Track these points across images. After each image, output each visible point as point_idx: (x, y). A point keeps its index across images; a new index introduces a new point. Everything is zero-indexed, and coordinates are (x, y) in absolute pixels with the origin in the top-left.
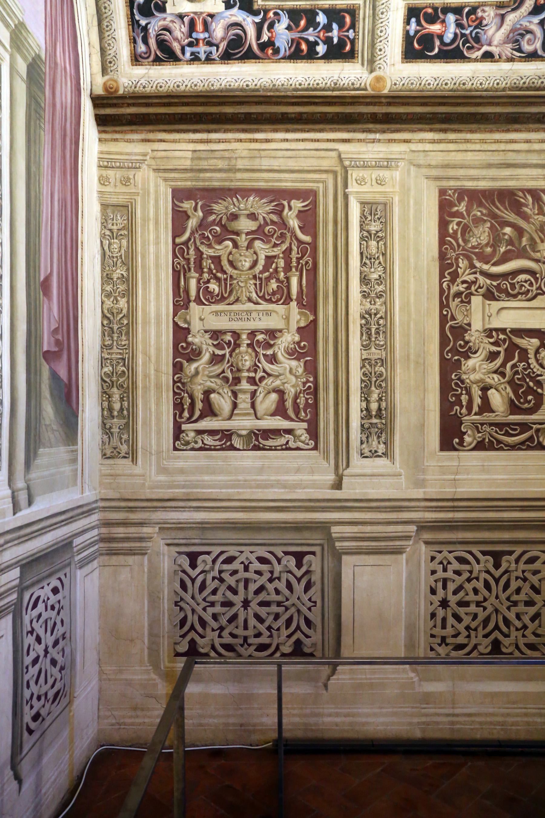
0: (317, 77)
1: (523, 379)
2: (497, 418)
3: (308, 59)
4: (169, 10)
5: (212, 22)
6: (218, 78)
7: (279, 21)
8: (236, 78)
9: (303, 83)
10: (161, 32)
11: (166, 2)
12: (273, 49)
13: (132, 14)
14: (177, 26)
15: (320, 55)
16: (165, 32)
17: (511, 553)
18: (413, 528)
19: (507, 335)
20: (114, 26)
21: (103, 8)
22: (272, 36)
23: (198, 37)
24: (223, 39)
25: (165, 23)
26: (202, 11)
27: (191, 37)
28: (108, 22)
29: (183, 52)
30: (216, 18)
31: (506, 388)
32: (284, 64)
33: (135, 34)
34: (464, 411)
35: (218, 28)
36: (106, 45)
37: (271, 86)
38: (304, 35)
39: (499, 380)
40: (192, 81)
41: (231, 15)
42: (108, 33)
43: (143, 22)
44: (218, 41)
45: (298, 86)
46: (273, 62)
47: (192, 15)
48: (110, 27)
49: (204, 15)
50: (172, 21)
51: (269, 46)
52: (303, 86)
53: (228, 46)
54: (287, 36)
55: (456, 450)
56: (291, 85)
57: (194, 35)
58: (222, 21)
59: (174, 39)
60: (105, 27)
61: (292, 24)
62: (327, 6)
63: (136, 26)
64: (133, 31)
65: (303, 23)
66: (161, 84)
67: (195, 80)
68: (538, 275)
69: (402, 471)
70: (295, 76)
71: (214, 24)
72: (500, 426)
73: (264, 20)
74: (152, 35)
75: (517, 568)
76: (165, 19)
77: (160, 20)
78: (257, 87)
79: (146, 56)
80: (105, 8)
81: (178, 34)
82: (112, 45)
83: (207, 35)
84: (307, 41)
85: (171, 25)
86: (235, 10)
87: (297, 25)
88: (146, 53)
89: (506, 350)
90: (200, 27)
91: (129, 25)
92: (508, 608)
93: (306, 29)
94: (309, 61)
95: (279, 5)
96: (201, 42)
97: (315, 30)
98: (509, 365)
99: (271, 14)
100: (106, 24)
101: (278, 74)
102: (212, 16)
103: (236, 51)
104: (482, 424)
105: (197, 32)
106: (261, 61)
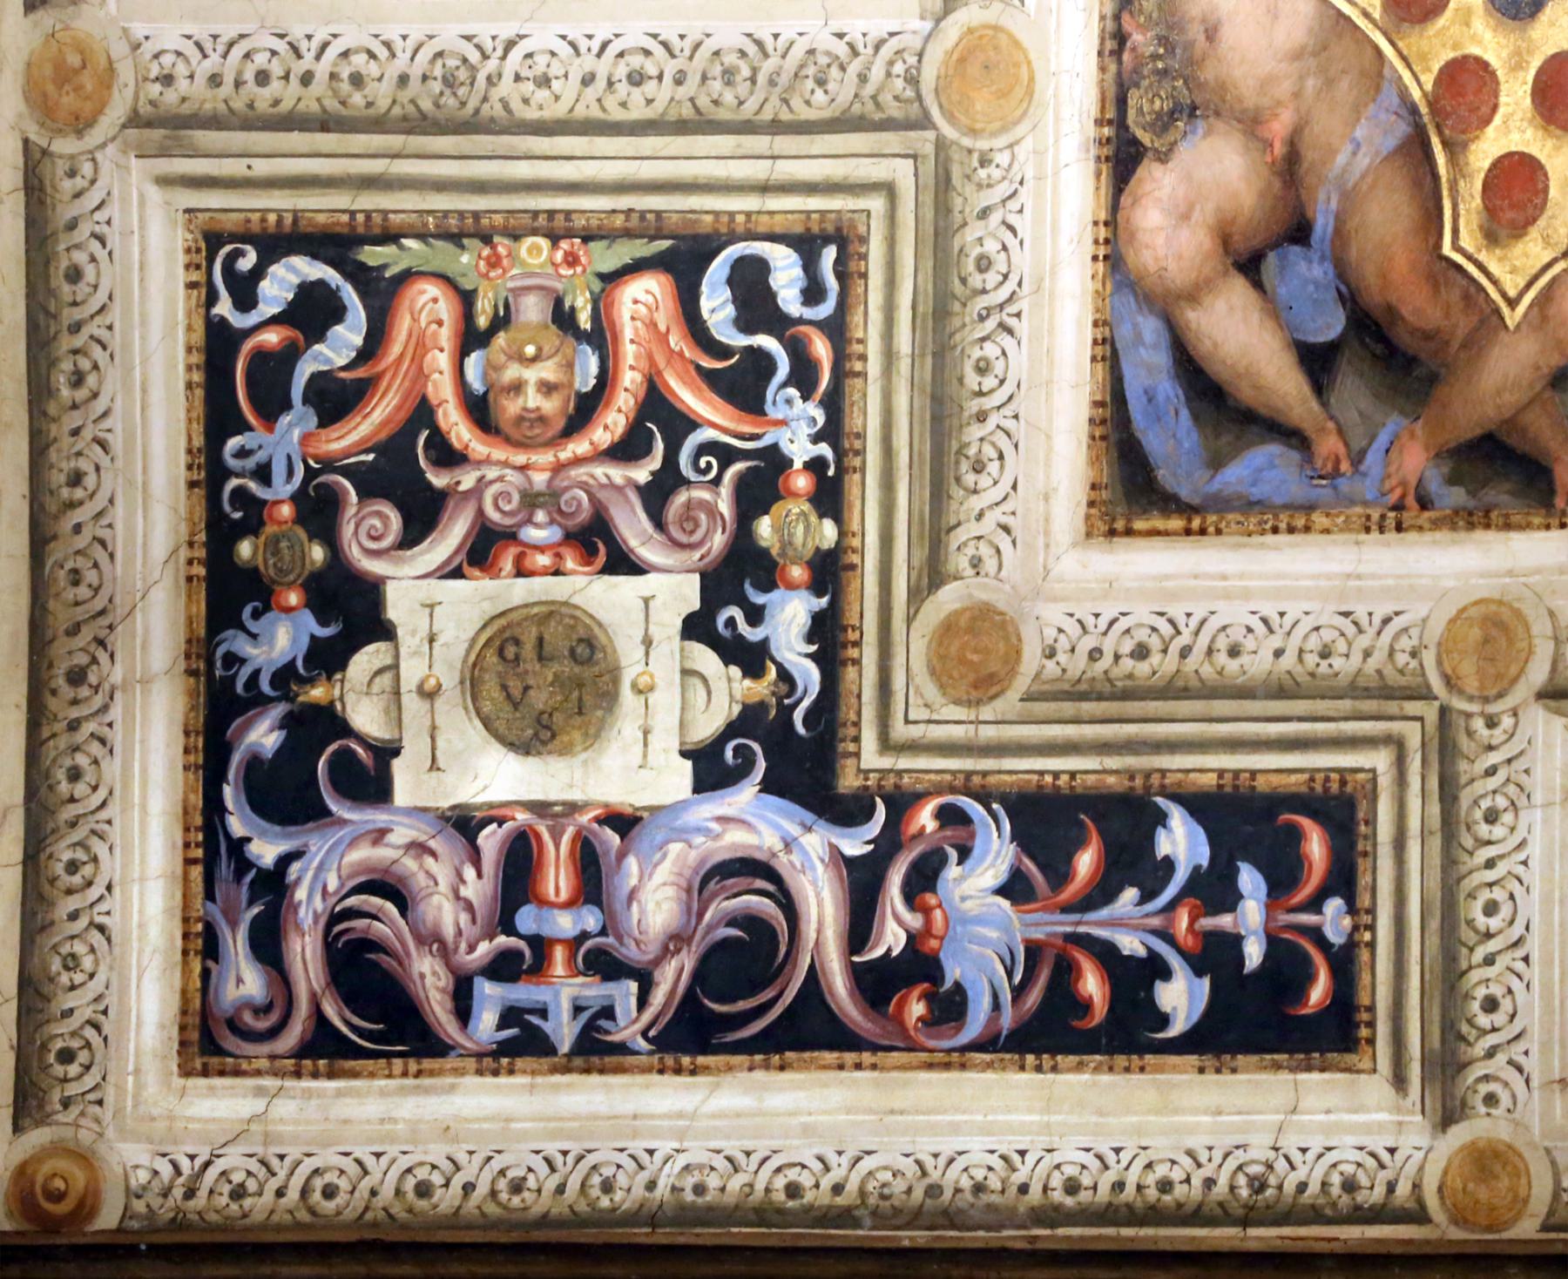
0: (1161, 1147)
3: (1111, 1051)
4: (402, 794)
5: (622, 855)
6: (637, 1146)
7: (964, 853)
8: (733, 1147)
9: (1086, 1181)
10: (352, 901)
11: (396, 752)
12: (929, 997)
13: (214, 808)
14: (442, 871)
15: (1176, 1029)
16: (376, 901)
20: (110, 866)
21: (61, 775)
22: (928, 930)
23: (546, 931)
24: (676, 941)
25: (383, 853)
26: (576, 795)
27: (509, 928)
28: (81, 844)
29: (463, 1010)
30: (646, 836)
32: (990, 1076)
33: (215, 911)
35: (651, 885)
36: (56, 965)
37: (918, 1194)
38: (1094, 924)
40: (496, 1165)
41: (721, 819)
42: (72, 903)
43: (265, 851)
44: (652, 951)
45: (1058, 1196)
46: (930, 1066)
47: (522, 817)
48: (87, 870)
49: (585, 818)
50: (419, 848)
51: (910, 982)
52: (1085, 1196)
53: (698, 976)
54: (1007, 929)
56: (1024, 1189)
57: (527, 918)
58: (675, 848)
59: (421, 940)
60: (59, 869)
61: (1030, 866)
62: (1210, 780)
63: (225, 869)
64: (210, 895)
65: (1086, 862)
66: (330, 1177)
67: (517, 1159)
70: (1044, 1141)
71: (632, 863)
73: (888, 845)
74: (305, 916)
76: (379, 835)
77: (353, 843)
78: (840, 1201)
79: (263, 1024)
80: (75, 775)
81: (443, 913)
82: (87, 963)
83: (591, 919)
84: (1107, 955)
85: (410, 864)
86: (744, 797)
87: (1059, 874)
88: (267, 1009)
90: (557, 878)
91: (189, 862)
93: (1102, 892)
94: (1121, 1060)
95: (969, 774)
96: (559, 953)
97: (1146, 897)
99: (925, 818)
100: (67, 856)
101: (955, 1129)
102: (624, 822)
103: (742, 1005)
105: (543, 902)
106: (867, 1057)
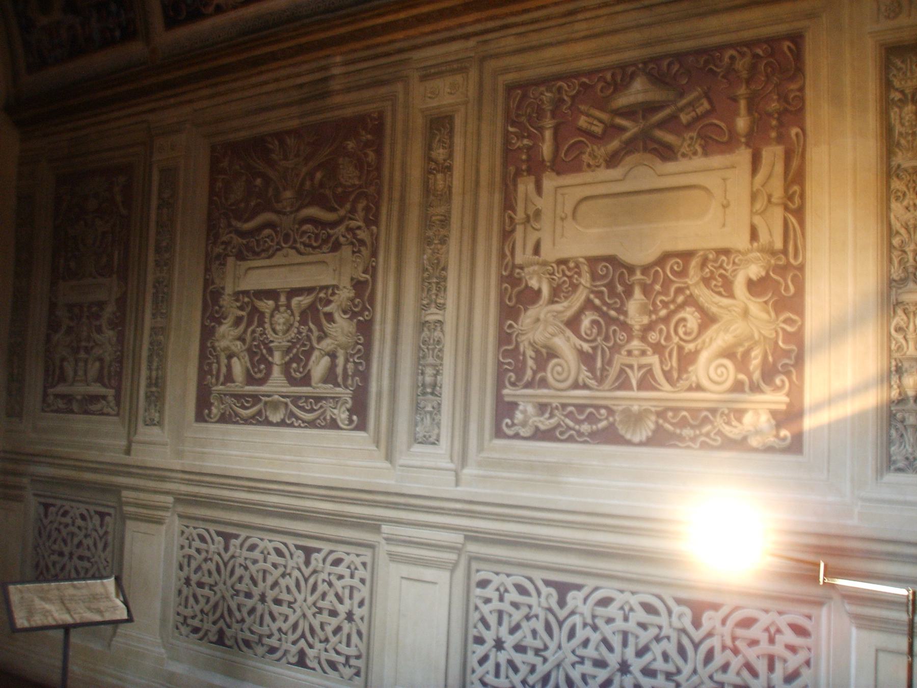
1: (258, 347)
2: (237, 389)
17: (579, 587)
18: (170, 499)
19: (249, 297)
31: (245, 356)
34: (214, 381)
39: (241, 348)
55: (206, 421)
68: (278, 229)
69: (168, 440)
72: (237, 397)
75: (323, 568)
89: (249, 314)
92: (314, 615)
98: (250, 330)
104: (225, 395)
